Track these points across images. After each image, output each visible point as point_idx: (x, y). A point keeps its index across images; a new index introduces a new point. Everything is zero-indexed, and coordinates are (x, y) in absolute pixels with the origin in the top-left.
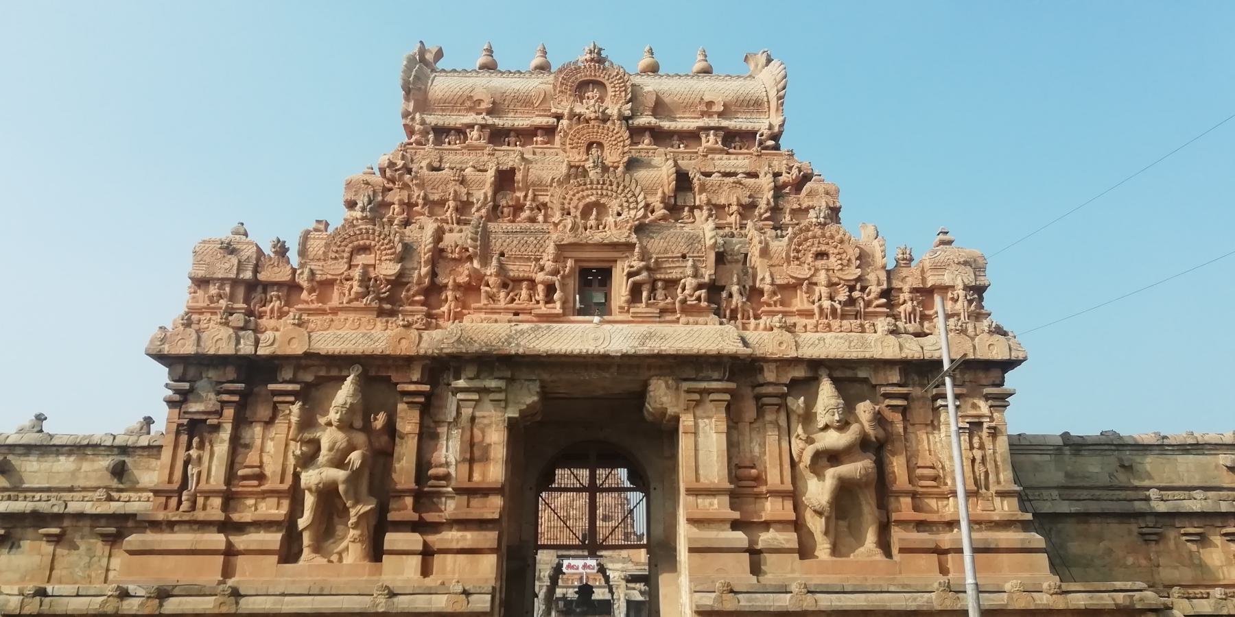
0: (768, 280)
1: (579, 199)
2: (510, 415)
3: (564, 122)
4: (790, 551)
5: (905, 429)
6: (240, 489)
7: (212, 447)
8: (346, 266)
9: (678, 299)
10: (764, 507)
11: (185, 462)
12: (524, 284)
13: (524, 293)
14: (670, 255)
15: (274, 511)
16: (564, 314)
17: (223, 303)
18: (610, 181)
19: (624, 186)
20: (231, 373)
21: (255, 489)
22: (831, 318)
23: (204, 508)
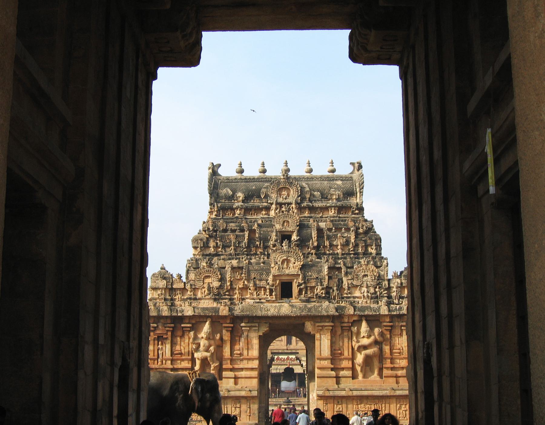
0: (347, 285)
1: (280, 258)
2: (260, 334)
3: (274, 206)
4: (349, 377)
5: (391, 337)
6: (175, 358)
7: (165, 344)
8: (203, 283)
9: (315, 294)
10: (343, 362)
11: (158, 349)
12: (263, 289)
13: (263, 292)
14: (312, 277)
15: (187, 365)
16: (276, 300)
17: (163, 296)
18: (291, 251)
19: (296, 253)
20: (169, 321)
21: (180, 358)
22: (367, 299)
23: (166, 364)
